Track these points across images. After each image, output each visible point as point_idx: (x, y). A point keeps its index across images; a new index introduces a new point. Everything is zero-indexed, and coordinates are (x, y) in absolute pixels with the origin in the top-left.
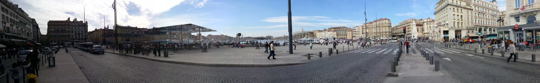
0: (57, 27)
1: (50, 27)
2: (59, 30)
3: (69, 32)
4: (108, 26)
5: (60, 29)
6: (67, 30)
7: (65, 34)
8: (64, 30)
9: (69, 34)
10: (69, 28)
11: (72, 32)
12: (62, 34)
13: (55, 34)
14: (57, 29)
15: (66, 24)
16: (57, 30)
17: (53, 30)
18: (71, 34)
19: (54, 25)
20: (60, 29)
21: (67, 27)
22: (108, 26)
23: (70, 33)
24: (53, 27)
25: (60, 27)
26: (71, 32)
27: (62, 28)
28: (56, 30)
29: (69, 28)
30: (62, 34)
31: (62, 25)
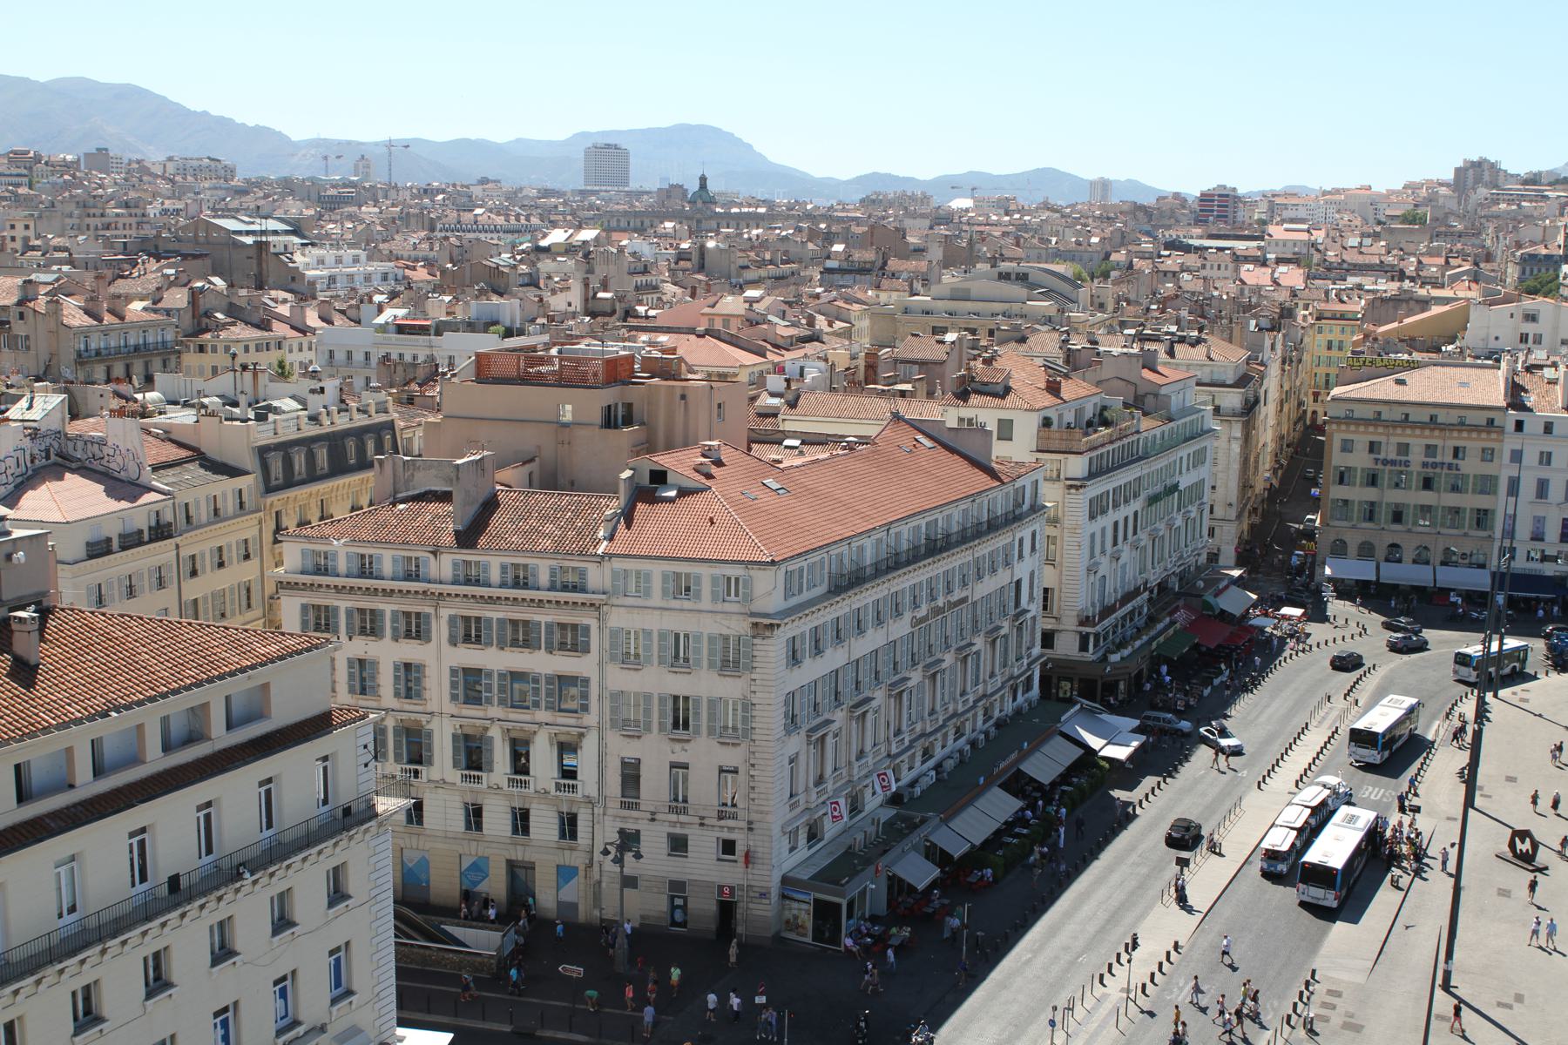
0: (1395, 440)
2: (1407, 463)
3: (1487, 485)
5: (1416, 456)
6: (1471, 466)
7: (1451, 500)
8: (1450, 466)
9: (1482, 502)
10: (1488, 455)
11: (1514, 487)
12: (1427, 498)
13: (1371, 494)
14: (1392, 456)
16: (1393, 463)
18: (1500, 503)
19: (1377, 420)
20: (1416, 456)
21: (1473, 444)
25: (1417, 443)
27: (1430, 450)
28: (1385, 462)
30: (1427, 498)
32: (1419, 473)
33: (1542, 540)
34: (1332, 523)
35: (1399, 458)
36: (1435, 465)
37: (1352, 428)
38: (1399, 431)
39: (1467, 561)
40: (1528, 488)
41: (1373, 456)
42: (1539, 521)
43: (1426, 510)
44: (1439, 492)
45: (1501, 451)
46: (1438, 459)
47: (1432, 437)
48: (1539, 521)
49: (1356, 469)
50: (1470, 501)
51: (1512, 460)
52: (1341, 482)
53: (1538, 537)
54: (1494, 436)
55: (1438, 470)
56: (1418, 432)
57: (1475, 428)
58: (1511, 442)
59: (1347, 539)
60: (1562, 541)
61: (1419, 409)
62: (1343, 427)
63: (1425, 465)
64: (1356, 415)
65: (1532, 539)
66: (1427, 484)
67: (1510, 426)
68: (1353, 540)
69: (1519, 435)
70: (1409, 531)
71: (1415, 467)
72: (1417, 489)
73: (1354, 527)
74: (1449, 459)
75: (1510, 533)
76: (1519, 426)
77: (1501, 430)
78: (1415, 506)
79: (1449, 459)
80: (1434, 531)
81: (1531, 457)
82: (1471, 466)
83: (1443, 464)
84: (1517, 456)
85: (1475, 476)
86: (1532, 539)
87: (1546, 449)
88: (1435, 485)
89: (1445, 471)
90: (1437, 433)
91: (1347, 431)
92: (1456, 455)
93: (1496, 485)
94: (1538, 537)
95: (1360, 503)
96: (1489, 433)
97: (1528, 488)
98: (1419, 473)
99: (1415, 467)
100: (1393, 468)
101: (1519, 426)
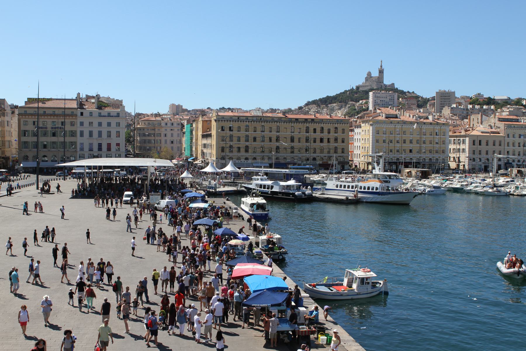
1: (22, 120)
2: (46, 128)
3: (73, 134)
4: (381, 72)
5: (49, 126)
8: (60, 128)
9: (72, 139)
10: (72, 124)
11: (82, 134)
12: (54, 139)
15: (56, 113)
17: (31, 127)
18: (79, 140)
20: (49, 126)
22: (381, 72)
23: (76, 136)
24: (31, 120)
26: (78, 134)
29: (72, 124)
30: (54, 139)
31: (54, 115)
32: (50, 131)
33: (93, 151)
34: (22, 150)
35: (43, 126)
36: (55, 128)
37: (27, 117)
38: (43, 117)
39: (69, 160)
40: (86, 134)
41: (34, 126)
42: (91, 145)
43: (54, 143)
44: (58, 137)
45: (77, 122)
46: (57, 126)
47: (54, 119)
48: (91, 145)
49: (29, 131)
50: (68, 139)
51: (81, 125)
52: (25, 136)
53: (91, 150)
54: (74, 117)
55: (57, 130)
56: (49, 117)
57: (69, 115)
58: (80, 119)
59: (28, 154)
60: (99, 151)
61: (49, 110)
62: (24, 117)
63: (52, 128)
64: (28, 112)
65: (89, 151)
66: (54, 135)
67: (79, 114)
68: (31, 155)
69: (82, 117)
70: (49, 151)
71: (49, 129)
72: (51, 136)
73: (30, 150)
74: (60, 126)
75: (82, 149)
76: (82, 114)
77: (76, 115)
78: (50, 142)
79: (60, 126)
80: (57, 150)
81: (86, 124)
82: (68, 128)
83: (58, 127)
84: (82, 124)
85: (69, 131)
86: (89, 151)
87: (91, 121)
88: (56, 135)
89: (59, 130)
90: (55, 117)
91: (25, 118)
92: (62, 125)
93: (76, 134)
94: (91, 150)
95: (32, 142)
96: (72, 116)
97: (86, 134)
98: (50, 131)
99: (49, 129)
100: (42, 130)
101: (82, 114)
